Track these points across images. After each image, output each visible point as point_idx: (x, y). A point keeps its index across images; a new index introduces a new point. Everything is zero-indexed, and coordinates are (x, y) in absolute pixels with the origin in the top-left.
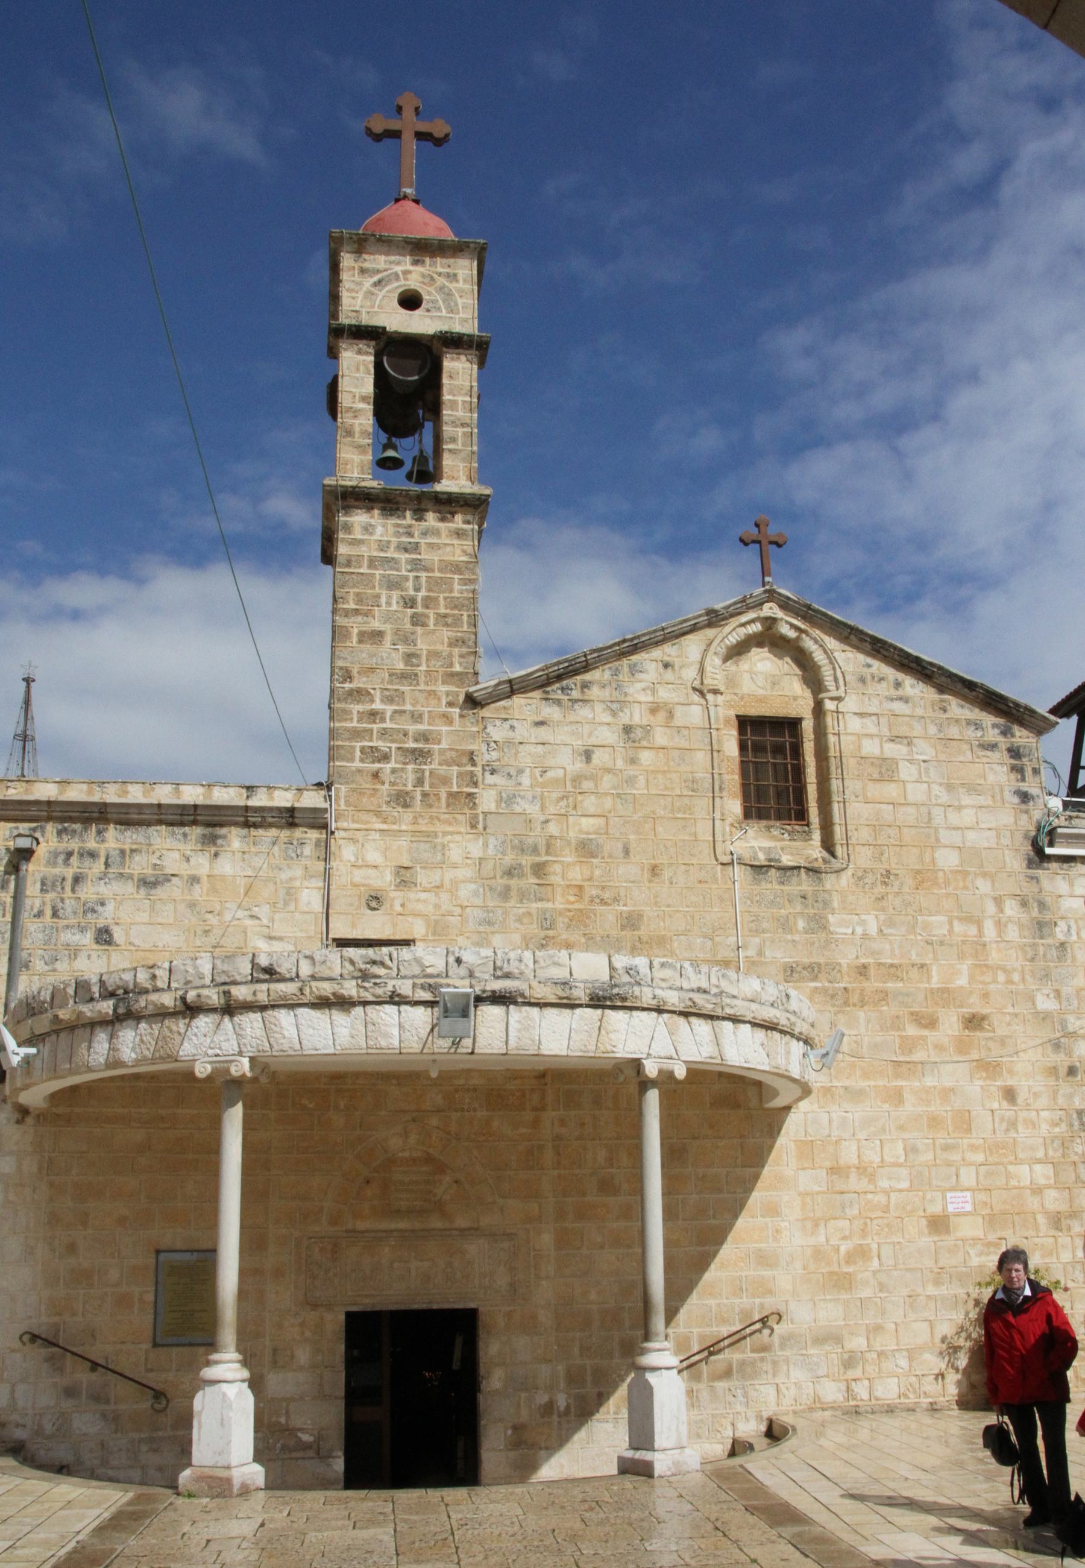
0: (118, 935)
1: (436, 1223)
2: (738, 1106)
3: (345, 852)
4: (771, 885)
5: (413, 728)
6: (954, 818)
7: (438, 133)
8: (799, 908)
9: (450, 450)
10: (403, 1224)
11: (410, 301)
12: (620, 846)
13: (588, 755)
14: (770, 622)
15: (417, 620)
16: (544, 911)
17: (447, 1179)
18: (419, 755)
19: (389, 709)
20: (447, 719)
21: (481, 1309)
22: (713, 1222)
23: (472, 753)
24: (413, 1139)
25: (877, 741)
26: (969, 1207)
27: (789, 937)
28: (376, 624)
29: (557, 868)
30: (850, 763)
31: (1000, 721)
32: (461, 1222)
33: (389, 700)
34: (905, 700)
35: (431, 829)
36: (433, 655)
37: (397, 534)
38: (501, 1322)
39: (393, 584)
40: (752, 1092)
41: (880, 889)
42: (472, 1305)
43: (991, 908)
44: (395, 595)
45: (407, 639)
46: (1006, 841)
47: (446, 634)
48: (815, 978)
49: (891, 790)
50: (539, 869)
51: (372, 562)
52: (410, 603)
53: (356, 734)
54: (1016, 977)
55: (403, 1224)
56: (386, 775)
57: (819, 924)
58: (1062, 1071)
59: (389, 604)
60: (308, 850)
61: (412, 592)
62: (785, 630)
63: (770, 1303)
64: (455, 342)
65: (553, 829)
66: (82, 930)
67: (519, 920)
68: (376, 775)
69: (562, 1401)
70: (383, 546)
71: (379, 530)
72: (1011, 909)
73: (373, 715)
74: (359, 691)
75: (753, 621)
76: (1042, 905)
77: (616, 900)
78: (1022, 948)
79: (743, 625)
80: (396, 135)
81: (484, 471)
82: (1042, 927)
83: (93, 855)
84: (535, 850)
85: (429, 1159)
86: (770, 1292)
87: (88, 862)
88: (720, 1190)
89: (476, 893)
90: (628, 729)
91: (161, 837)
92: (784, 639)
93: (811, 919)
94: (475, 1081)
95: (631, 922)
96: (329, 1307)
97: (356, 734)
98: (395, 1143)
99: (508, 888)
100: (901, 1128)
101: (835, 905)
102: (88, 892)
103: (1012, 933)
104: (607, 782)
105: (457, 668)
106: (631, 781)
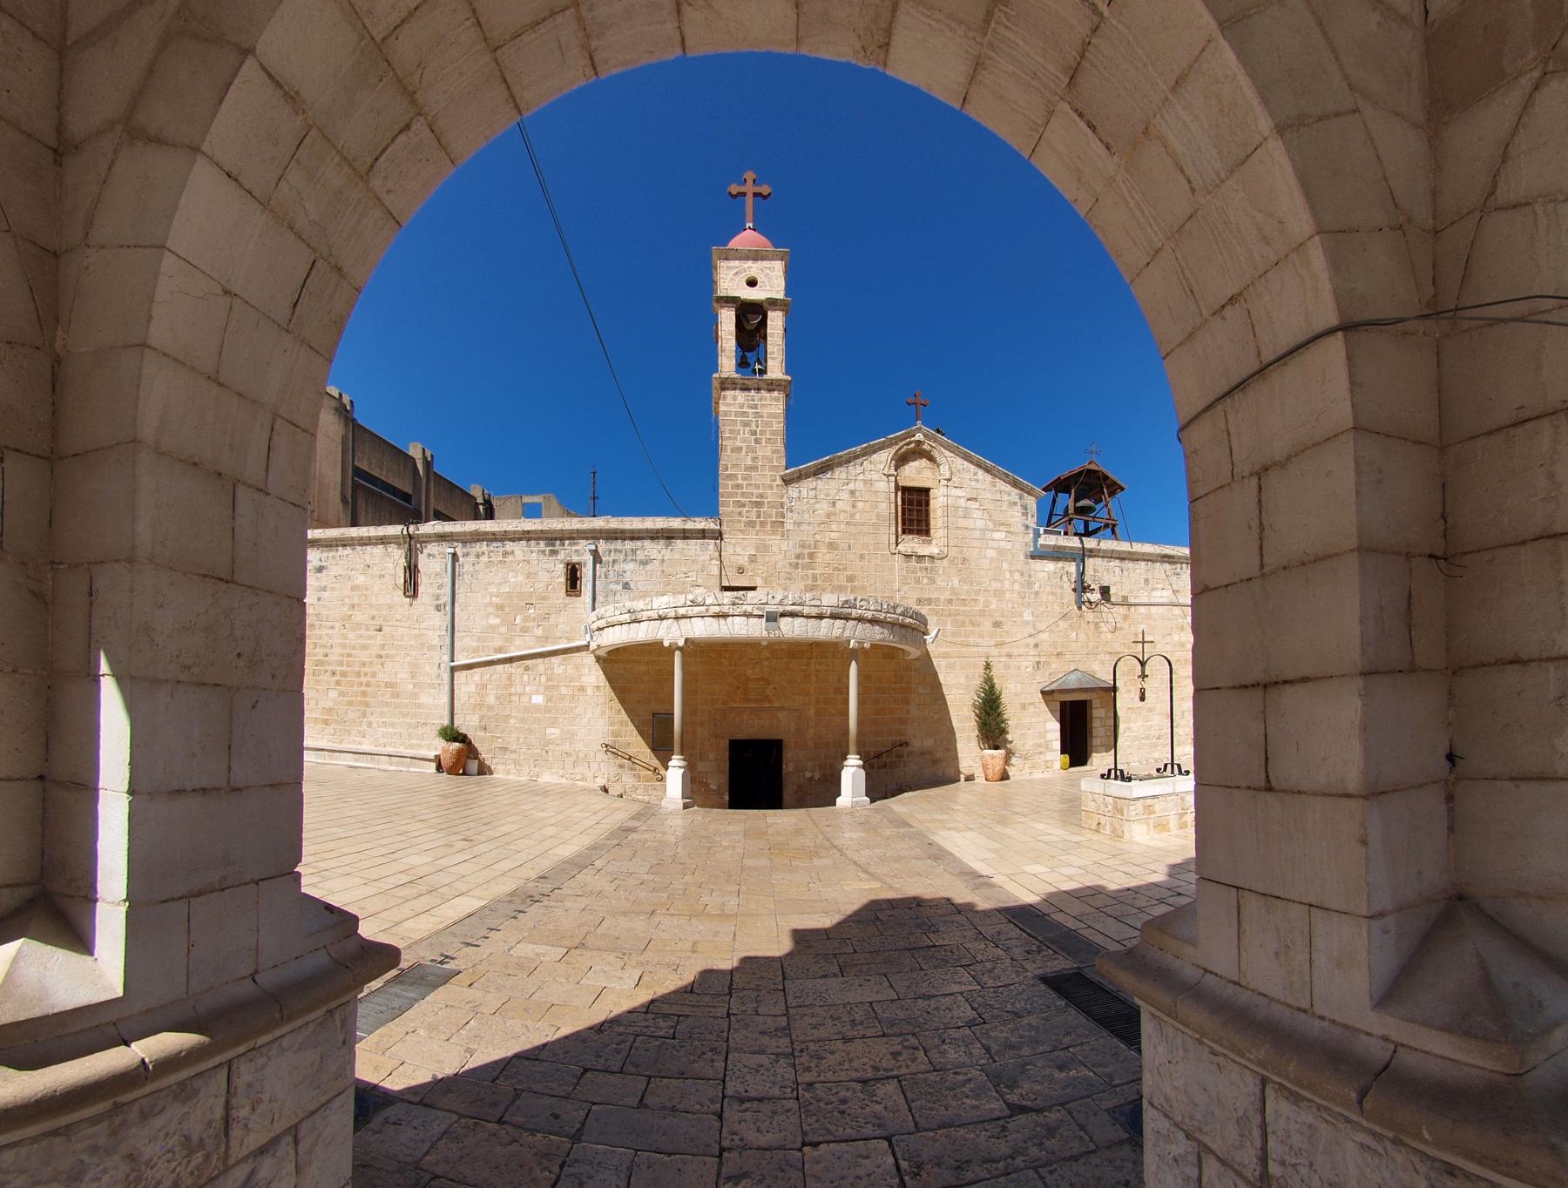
0: (632, 585)
1: (767, 705)
2: (893, 658)
3: (728, 550)
4: (913, 563)
5: (755, 492)
7: (765, 193)
8: (924, 574)
9: (772, 358)
10: (753, 705)
12: (847, 546)
13: (834, 504)
14: (919, 443)
15: (757, 441)
16: (813, 574)
17: (771, 687)
18: (758, 504)
19: (745, 483)
20: (771, 487)
21: (785, 740)
22: (881, 706)
23: (782, 503)
24: (756, 670)
28: (738, 444)
29: (819, 555)
31: (1018, 491)
32: (777, 705)
33: (745, 479)
34: (977, 481)
35: (763, 537)
36: (764, 457)
37: (747, 400)
38: (793, 745)
39: (746, 424)
40: (900, 652)
41: (960, 566)
42: (780, 738)
43: (1008, 575)
44: (747, 429)
45: (751, 450)
46: (1017, 546)
47: (769, 447)
48: (930, 605)
50: (811, 556)
51: (736, 414)
52: (754, 433)
53: (731, 495)
56: (744, 513)
57: (932, 580)
58: (1031, 646)
59: (744, 434)
60: (711, 547)
61: (754, 428)
62: (925, 447)
63: (903, 738)
65: (818, 537)
66: (618, 583)
67: (802, 578)
68: (740, 514)
69: (817, 776)
70: (742, 406)
71: (739, 397)
72: (1017, 576)
73: (738, 486)
74: (731, 475)
75: (910, 443)
76: (1030, 576)
77: (845, 569)
78: (1019, 593)
79: (907, 444)
80: (744, 194)
81: (790, 366)
82: (1030, 584)
83: (620, 551)
84: (809, 546)
85: (763, 679)
86: (903, 735)
87: (618, 554)
88: (884, 693)
89: (784, 566)
90: (852, 492)
91: (647, 543)
92: (925, 450)
93: (929, 578)
94: (783, 647)
95: (851, 579)
96: (723, 738)
97: (731, 495)
98: (749, 672)
100: (962, 668)
101: (941, 572)
102: (616, 567)
103: (1017, 587)
104: (842, 517)
105: (775, 464)
106: (852, 516)
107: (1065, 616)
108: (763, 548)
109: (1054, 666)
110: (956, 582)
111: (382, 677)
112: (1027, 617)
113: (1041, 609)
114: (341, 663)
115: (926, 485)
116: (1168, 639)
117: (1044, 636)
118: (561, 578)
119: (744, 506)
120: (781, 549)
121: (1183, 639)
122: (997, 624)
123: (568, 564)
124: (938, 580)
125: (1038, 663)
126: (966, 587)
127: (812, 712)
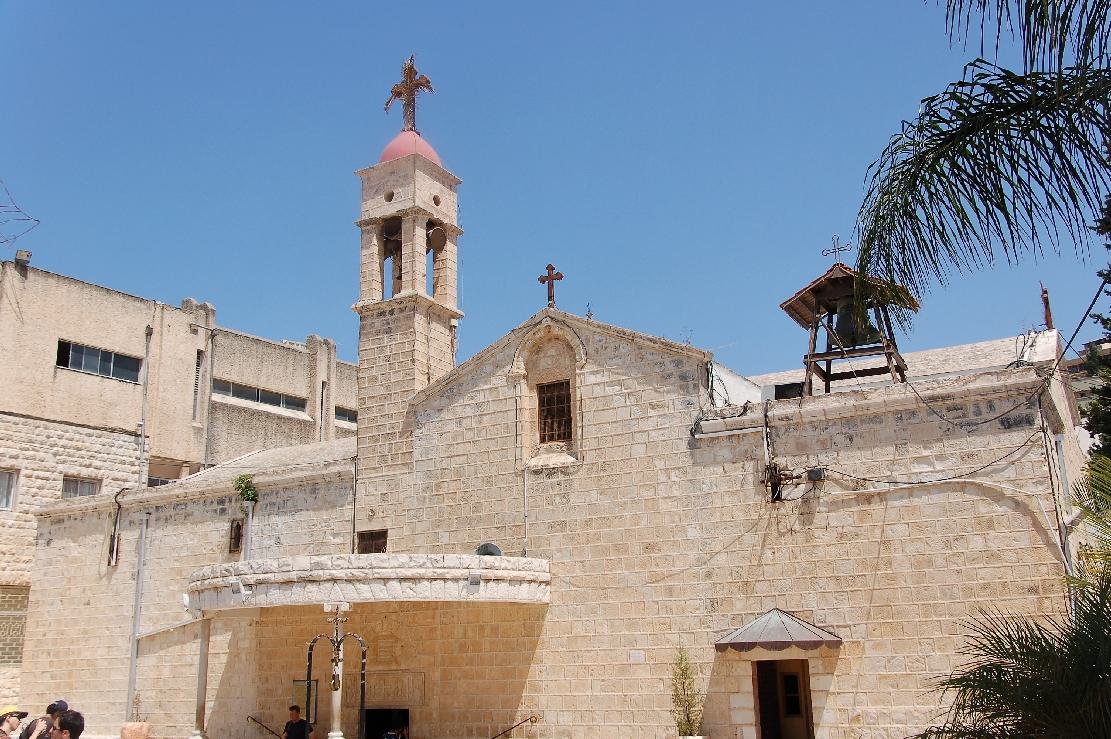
4: (543, 479)
6: (645, 425)
10: (381, 668)
11: (390, 197)
17: (399, 645)
25: (602, 386)
26: (642, 660)
27: (551, 507)
30: (587, 403)
32: (403, 667)
43: (662, 478)
49: (609, 416)
54: (677, 518)
55: (381, 668)
58: (702, 575)
64: (406, 213)
85: (392, 636)
88: (513, 650)
98: (378, 629)
99: (425, 498)
107: (753, 526)
108: (394, 484)
109: (739, 605)
110: (594, 493)
111: (86, 655)
112: (692, 533)
113: (717, 518)
114: (55, 644)
115: (560, 377)
116: (959, 548)
117: (722, 559)
118: (226, 540)
119: (377, 440)
120: (412, 481)
121: (994, 547)
122: (649, 548)
123: (233, 522)
124: (573, 498)
125: (713, 601)
126: (606, 502)
127: (436, 675)
